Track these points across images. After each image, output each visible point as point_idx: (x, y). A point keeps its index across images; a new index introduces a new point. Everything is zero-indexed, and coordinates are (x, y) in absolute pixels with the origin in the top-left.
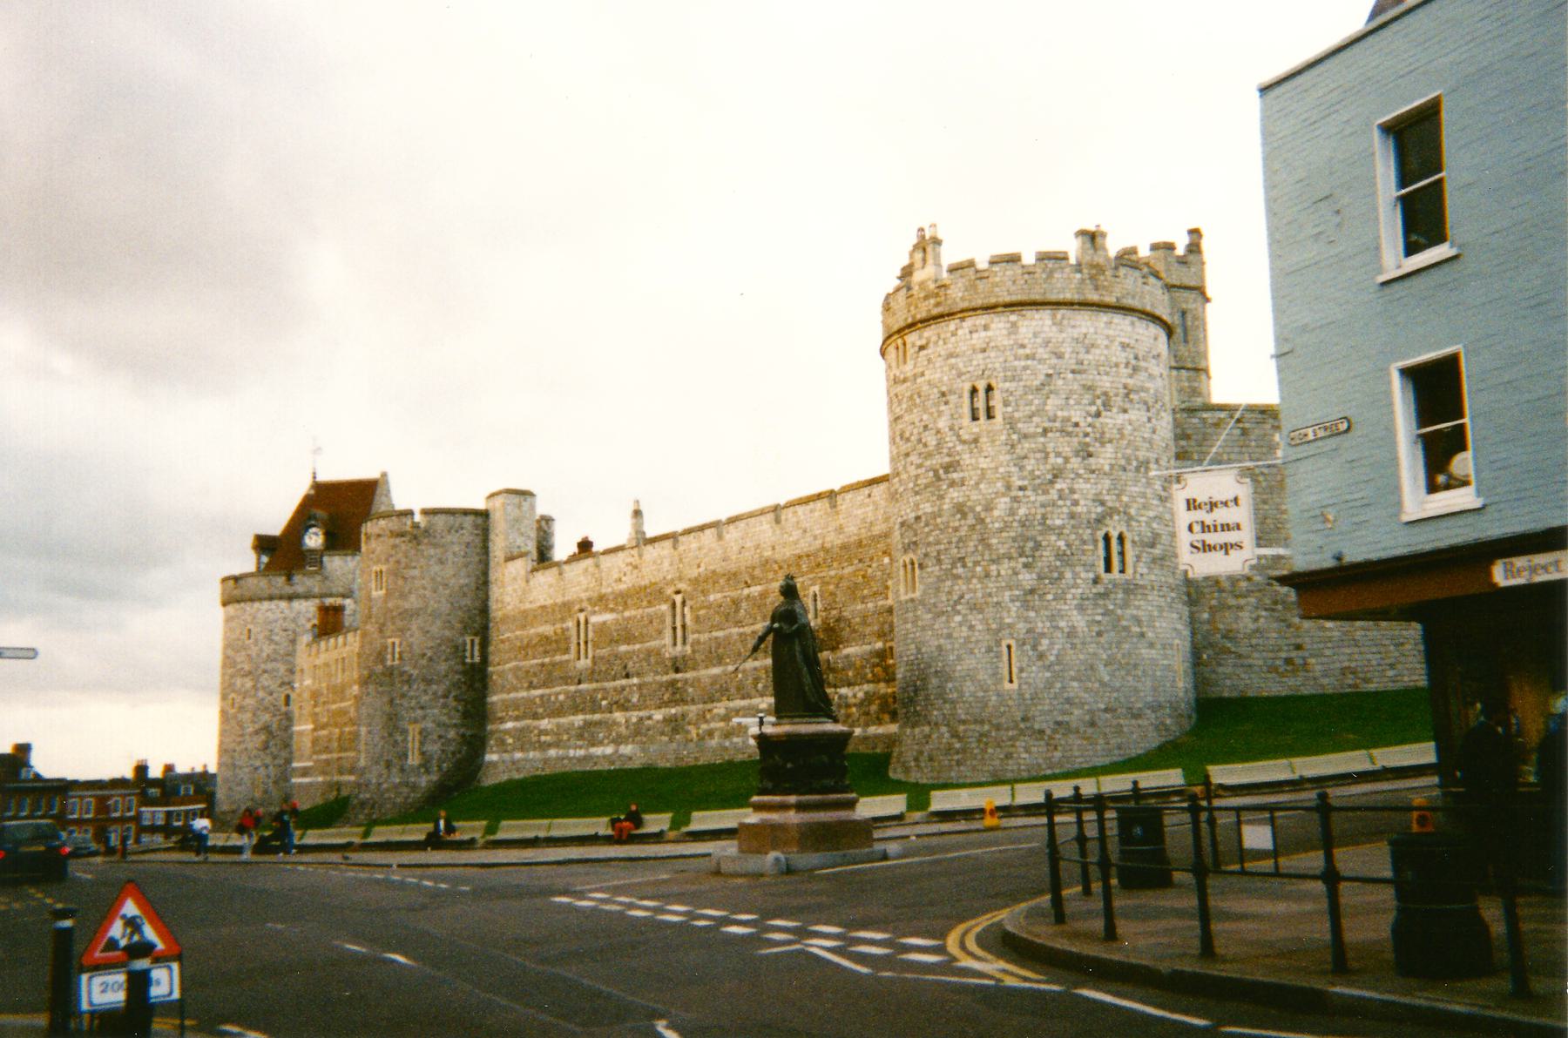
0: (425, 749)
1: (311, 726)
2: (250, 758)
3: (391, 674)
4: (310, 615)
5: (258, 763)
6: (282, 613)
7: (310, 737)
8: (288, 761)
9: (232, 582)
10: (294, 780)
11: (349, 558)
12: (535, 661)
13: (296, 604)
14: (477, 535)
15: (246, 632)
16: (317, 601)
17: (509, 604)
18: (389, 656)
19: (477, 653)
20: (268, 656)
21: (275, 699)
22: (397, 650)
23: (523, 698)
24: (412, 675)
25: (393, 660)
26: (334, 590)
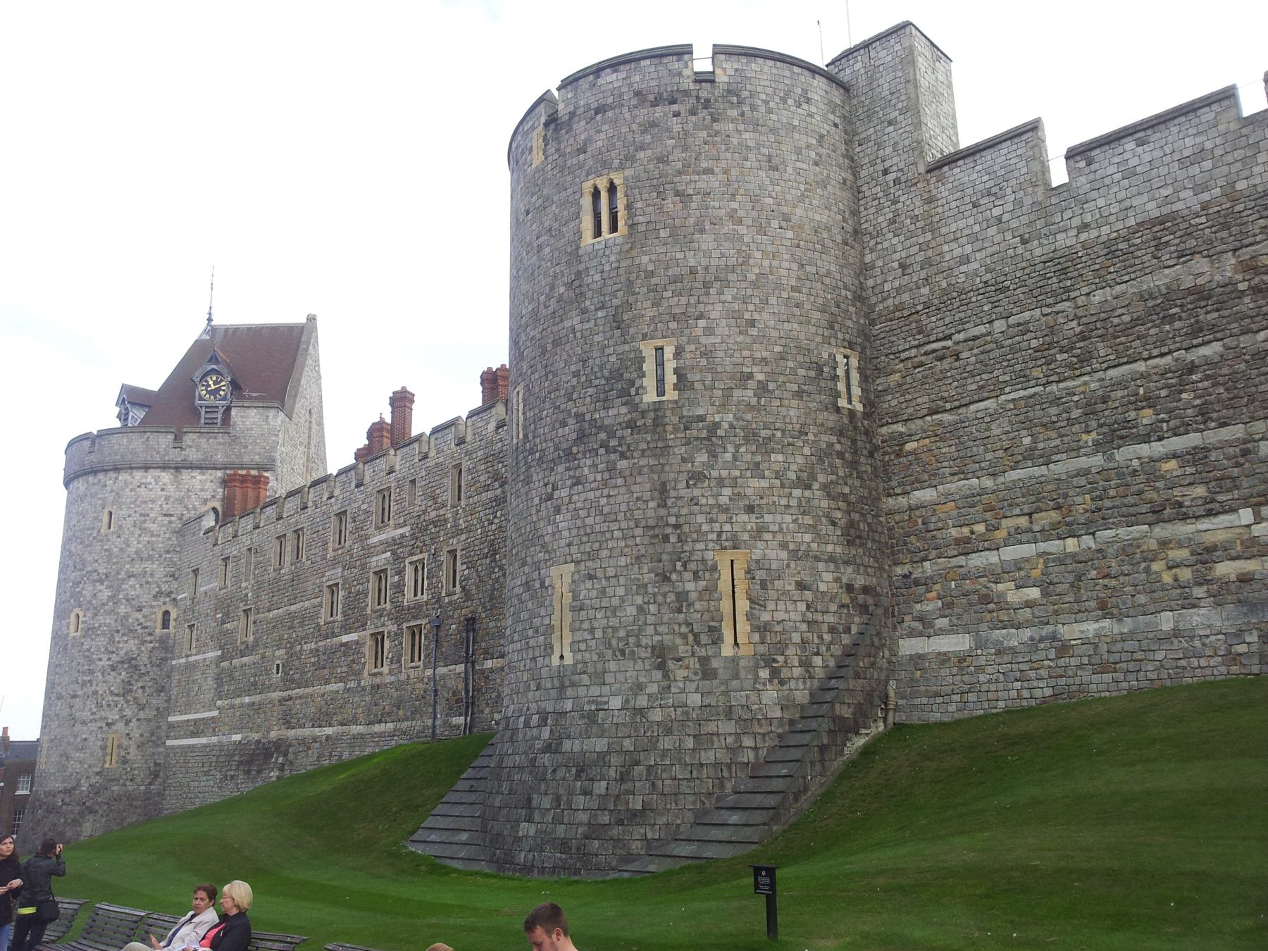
0: (766, 617)
1: (213, 654)
2: (99, 706)
3: (658, 423)
4: (207, 495)
5: (113, 716)
6: (163, 490)
7: (211, 672)
8: (162, 713)
9: (87, 444)
10: (169, 743)
11: (272, 413)
12: (1140, 367)
13: (185, 475)
14: (836, 125)
15: (105, 518)
16: (219, 474)
17: (966, 260)
18: (649, 382)
19: (856, 391)
20: (136, 552)
21: (144, 616)
22: (670, 366)
23: (1085, 472)
24: (717, 425)
25: (661, 393)
26: (246, 459)
